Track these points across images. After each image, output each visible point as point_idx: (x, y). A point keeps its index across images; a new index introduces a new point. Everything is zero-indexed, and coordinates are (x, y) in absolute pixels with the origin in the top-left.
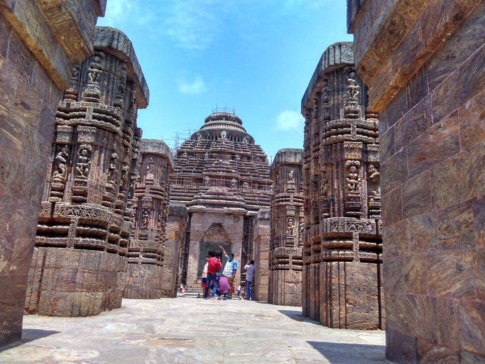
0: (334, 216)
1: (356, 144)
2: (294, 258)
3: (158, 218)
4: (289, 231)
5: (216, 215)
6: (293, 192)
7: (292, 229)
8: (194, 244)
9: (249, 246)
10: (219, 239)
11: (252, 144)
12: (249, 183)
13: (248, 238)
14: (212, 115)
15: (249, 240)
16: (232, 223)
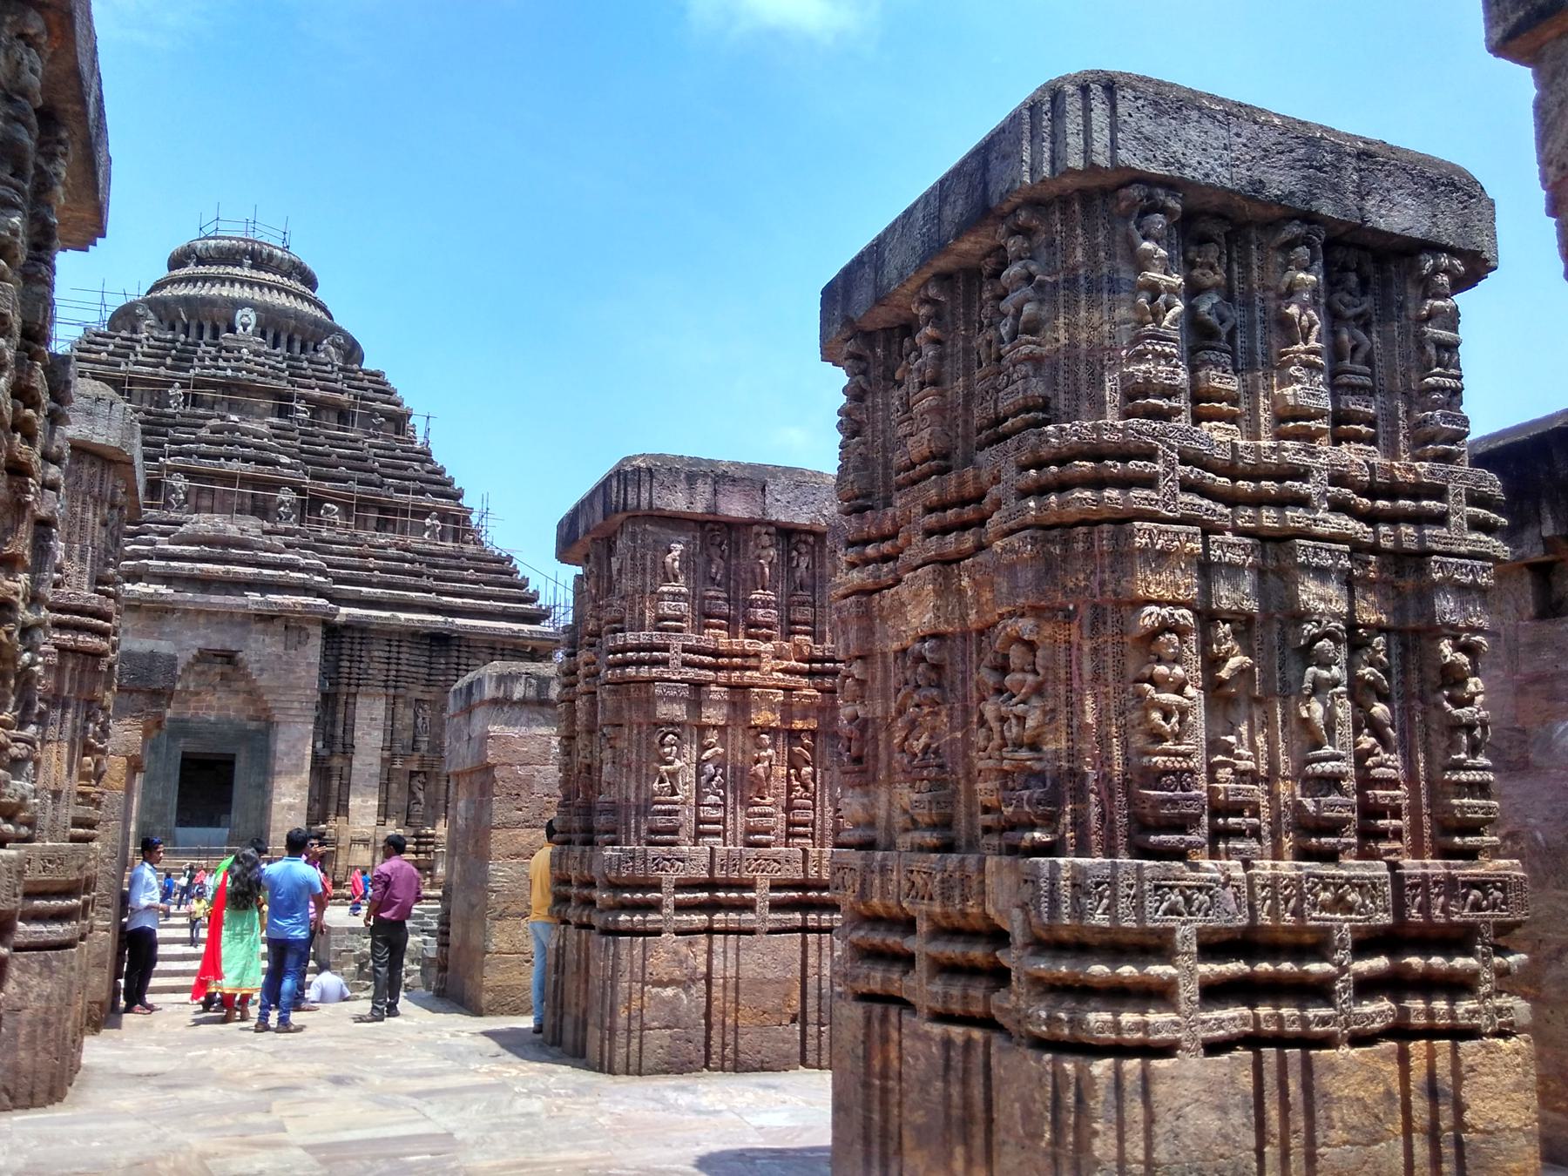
0: (1083, 849)
1: (1177, 534)
2: (681, 887)
3: (84, 738)
4: (662, 781)
5: (215, 619)
6: (679, 630)
7: (673, 775)
9: (339, 731)
10: (221, 708)
11: (355, 367)
12: (346, 510)
13: (336, 702)
14: (199, 245)
15: (341, 709)
16: (280, 649)
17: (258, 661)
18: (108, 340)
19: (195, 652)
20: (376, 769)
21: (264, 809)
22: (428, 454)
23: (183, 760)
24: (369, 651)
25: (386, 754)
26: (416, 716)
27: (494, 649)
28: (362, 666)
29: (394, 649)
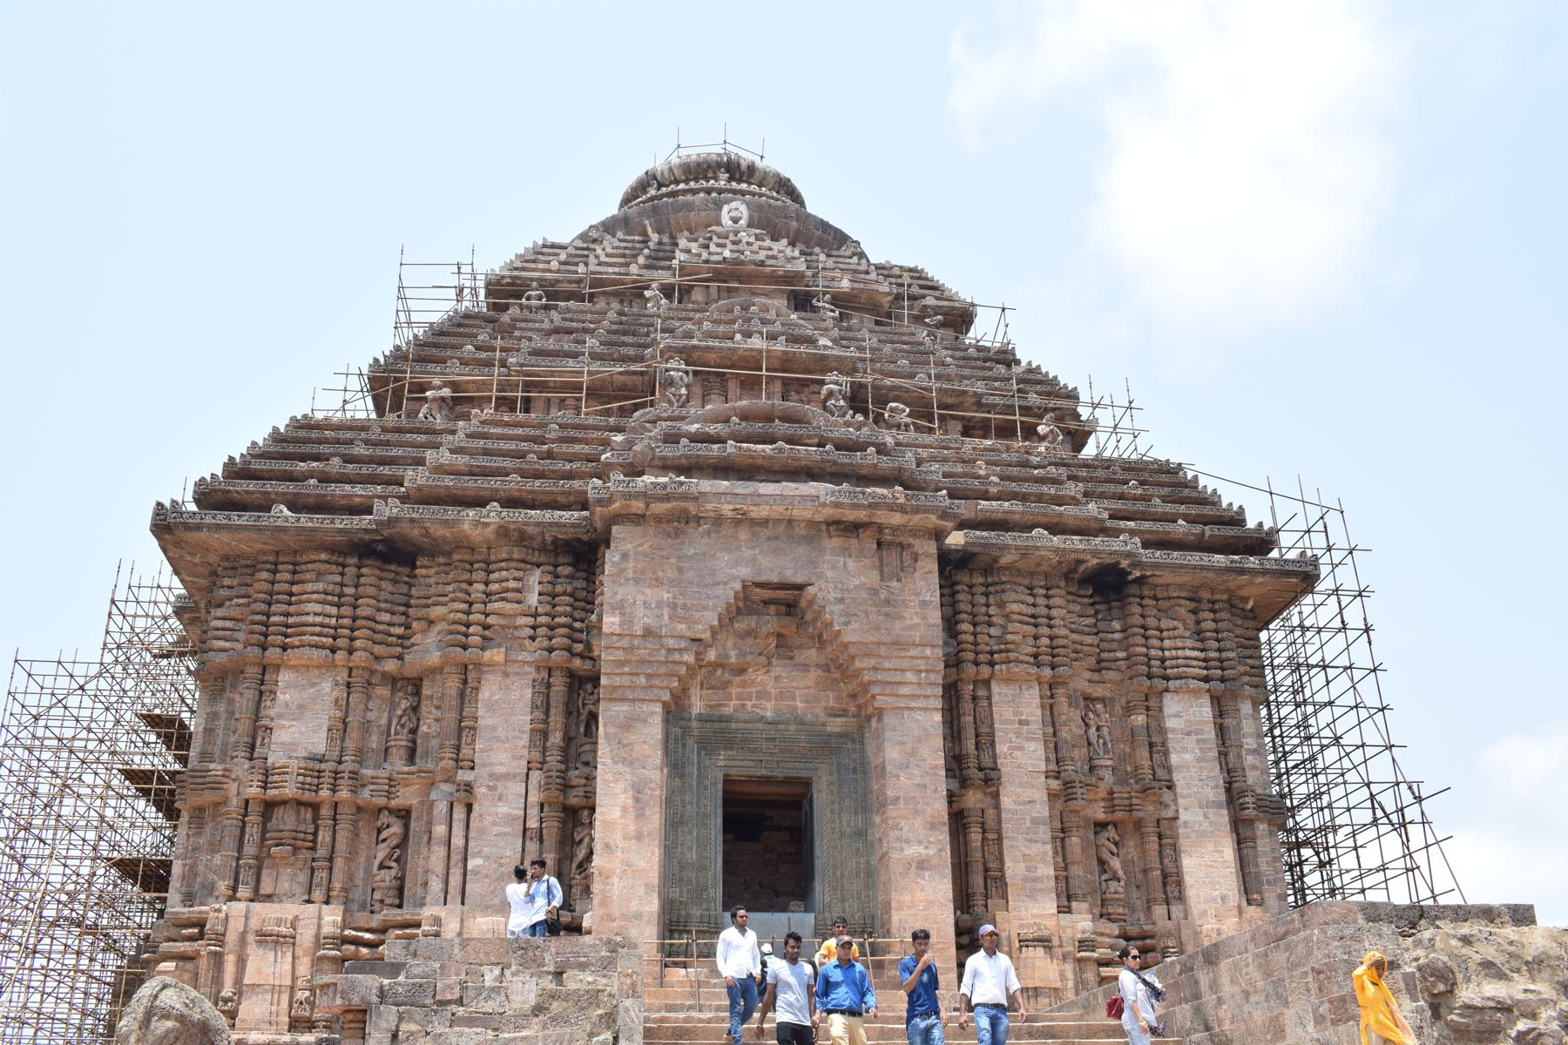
5: (765, 532)
8: (628, 724)
9: (970, 745)
10: (781, 696)
12: (922, 410)
15: (967, 706)
16: (873, 578)
17: (841, 600)
18: (558, 251)
19: (738, 586)
20: (1042, 810)
21: (871, 876)
22: (1013, 352)
23: (725, 792)
24: (1002, 605)
25: (1055, 784)
26: (1087, 725)
27: (1199, 601)
28: (993, 631)
29: (1041, 601)
